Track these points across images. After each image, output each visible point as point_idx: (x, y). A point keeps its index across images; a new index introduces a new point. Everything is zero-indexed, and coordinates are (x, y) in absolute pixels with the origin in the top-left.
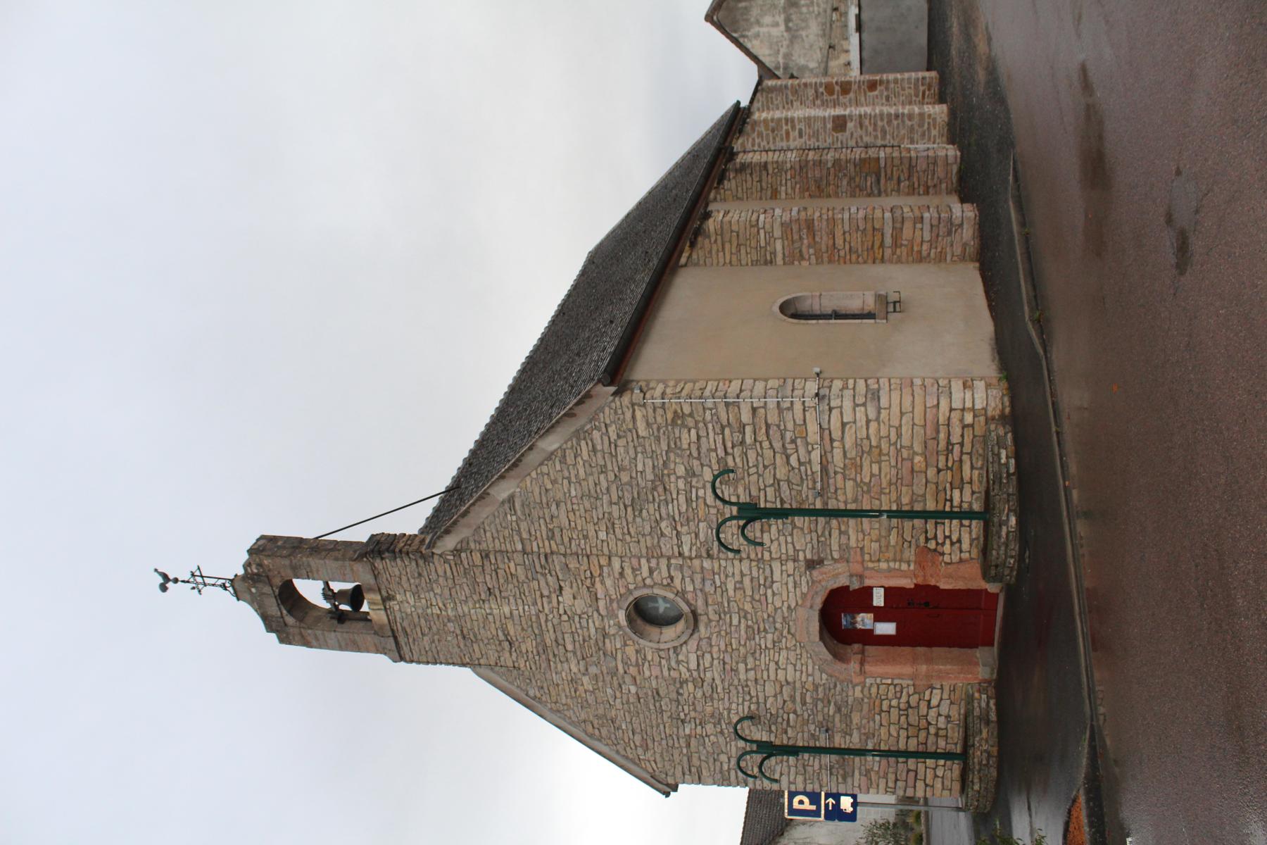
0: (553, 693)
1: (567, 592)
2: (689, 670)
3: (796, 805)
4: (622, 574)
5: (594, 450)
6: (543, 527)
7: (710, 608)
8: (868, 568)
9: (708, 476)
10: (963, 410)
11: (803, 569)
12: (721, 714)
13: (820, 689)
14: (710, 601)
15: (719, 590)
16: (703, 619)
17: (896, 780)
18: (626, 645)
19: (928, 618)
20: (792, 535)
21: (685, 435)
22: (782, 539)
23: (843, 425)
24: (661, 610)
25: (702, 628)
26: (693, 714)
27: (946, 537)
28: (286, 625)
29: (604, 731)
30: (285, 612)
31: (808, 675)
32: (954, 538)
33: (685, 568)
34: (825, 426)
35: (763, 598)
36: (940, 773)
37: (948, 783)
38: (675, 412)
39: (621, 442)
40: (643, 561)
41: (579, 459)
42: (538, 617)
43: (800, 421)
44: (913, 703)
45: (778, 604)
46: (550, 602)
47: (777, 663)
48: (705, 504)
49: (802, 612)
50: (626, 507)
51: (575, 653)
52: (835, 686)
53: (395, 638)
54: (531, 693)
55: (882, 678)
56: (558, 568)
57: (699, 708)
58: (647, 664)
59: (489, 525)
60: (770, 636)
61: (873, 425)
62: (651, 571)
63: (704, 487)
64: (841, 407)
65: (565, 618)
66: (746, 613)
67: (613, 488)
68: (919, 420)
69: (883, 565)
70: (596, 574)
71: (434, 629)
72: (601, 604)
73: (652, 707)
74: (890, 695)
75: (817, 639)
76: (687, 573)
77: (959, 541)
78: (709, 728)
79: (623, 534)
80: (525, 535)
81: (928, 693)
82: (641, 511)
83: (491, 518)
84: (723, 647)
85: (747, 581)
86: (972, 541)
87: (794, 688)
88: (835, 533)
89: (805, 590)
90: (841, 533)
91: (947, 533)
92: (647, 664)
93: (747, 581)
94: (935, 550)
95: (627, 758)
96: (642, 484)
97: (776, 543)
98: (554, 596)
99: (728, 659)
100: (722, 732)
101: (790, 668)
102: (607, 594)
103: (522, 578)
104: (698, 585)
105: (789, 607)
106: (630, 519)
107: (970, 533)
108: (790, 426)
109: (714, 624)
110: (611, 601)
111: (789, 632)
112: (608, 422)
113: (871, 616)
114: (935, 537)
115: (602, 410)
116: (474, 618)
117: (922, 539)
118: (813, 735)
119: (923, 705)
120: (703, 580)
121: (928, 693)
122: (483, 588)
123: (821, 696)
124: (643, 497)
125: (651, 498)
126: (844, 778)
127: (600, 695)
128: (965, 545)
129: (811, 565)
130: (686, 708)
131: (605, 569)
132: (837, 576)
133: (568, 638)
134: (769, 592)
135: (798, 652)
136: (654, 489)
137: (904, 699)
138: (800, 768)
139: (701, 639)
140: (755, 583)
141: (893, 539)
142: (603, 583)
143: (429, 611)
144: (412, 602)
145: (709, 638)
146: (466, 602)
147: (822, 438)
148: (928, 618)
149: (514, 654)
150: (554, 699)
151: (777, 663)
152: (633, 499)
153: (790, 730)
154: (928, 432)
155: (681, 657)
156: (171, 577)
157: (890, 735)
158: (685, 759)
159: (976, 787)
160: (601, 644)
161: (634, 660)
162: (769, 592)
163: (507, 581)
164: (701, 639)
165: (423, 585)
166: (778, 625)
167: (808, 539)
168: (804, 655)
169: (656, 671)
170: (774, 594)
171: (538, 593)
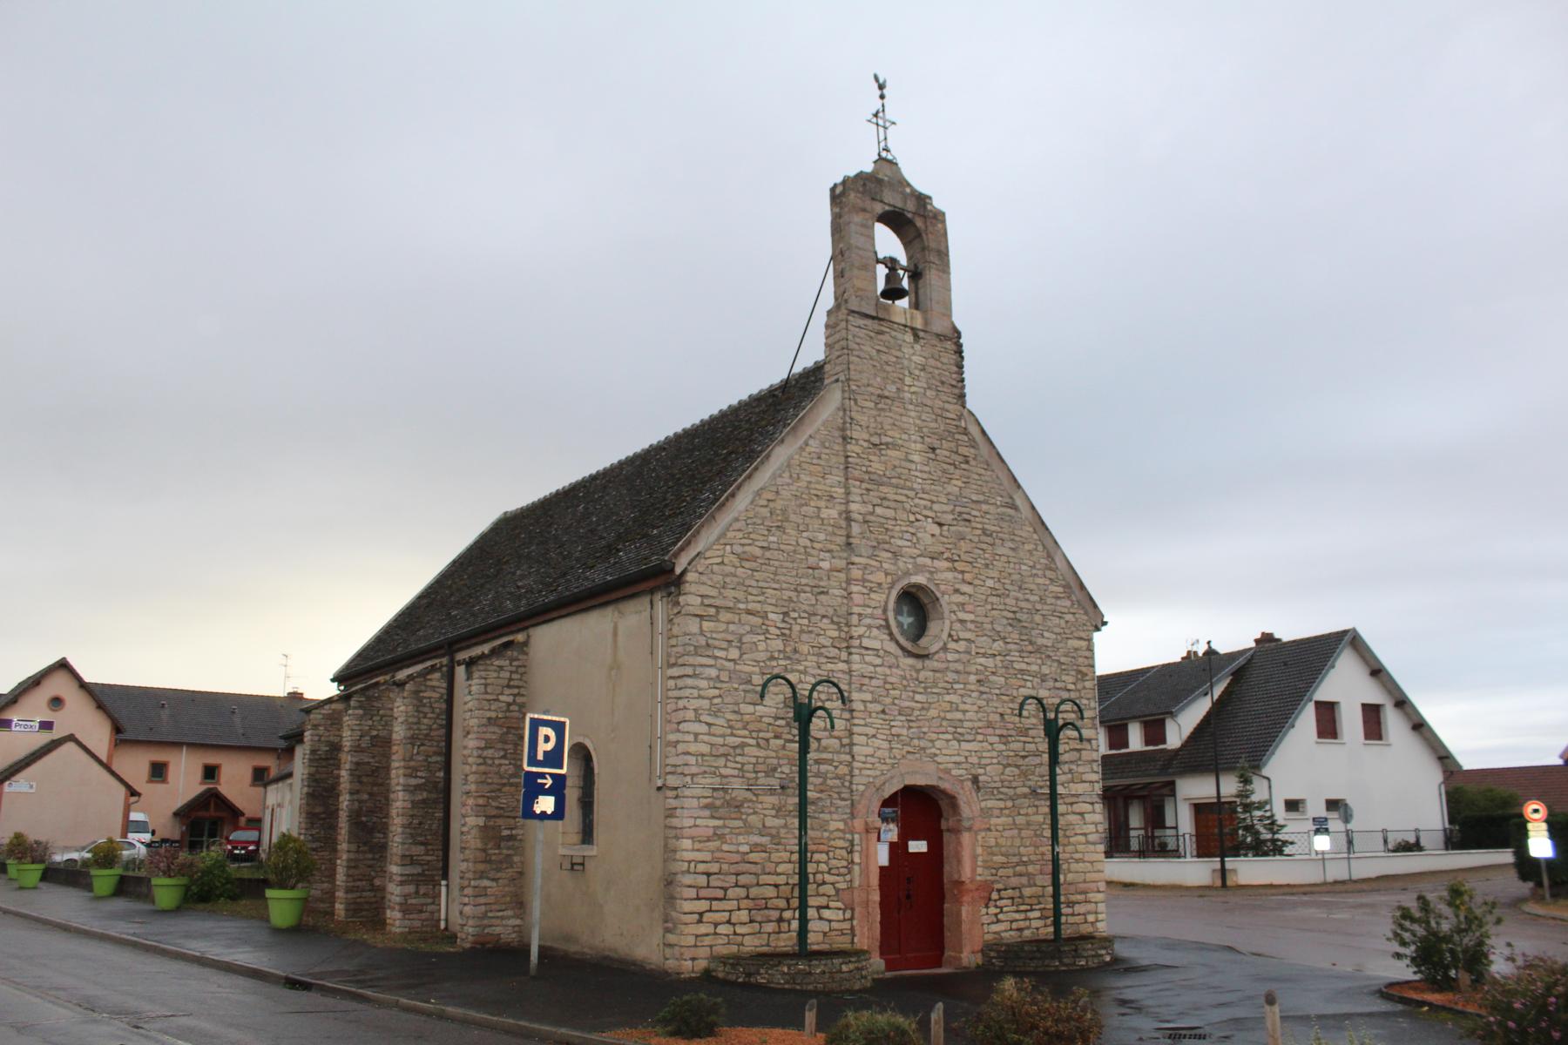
0: (812, 468)
1: (936, 530)
2: (860, 637)
4: (957, 591)
8: (976, 833)
9: (1042, 693)
12: (799, 662)
16: (918, 664)
17: (708, 874)
19: (917, 895)
21: (1071, 679)
22: (995, 754)
23: (1081, 814)
24: (910, 620)
25: (911, 661)
26: (796, 628)
29: (765, 512)
36: (722, 929)
37: (707, 941)
40: (971, 617)
42: (912, 489)
43: (1085, 777)
44: (822, 889)
49: (932, 768)
51: (872, 513)
54: (811, 442)
57: (805, 637)
60: (904, 732)
62: (962, 622)
65: (912, 518)
68: (1089, 877)
69: (979, 850)
71: (888, 369)
72: (928, 561)
73: (804, 581)
74: (834, 862)
75: (908, 782)
76: (965, 657)
77: (998, 921)
78: (777, 644)
80: (984, 507)
81: (839, 905)
85: (959, 715)
87: (839, 752)
88: (1001, 804)
89: (954, 772)
93: (959, 715)
96: (1034, 632)
99: (874, 682)
100: (772, 658)
101: (869, 750)
102: (937, 571)
103: (950, 489)
104: (953, 666)
106: (1005, 613)
108: (1081, 769)
115: (1086, 613)
117: (1000, 886)
118: (775, 770)
119: (822, 901)
120: (957, 672)
121: (839, 905)
122: (936, 444)
126: (706, 807)
127: (816, 524)
128: (995, 928)
129: (975, 780)
130: (805, 622)
132: (970, 805)
134: (949, 737)
136: (1031, 643)
137: (828, 878)
138: (722, 750)
141: (1000, 859)
142: (949, 570)
144: (914, 358)
148: (917, 895)
150: (805, 466)
153: (780, 742)
155: (875, 632)
157: (778, 864)
159: (844, 968)
161: (870, 577)
162: (949, 737)
163: (944, 471)
166: (916, 742)
169: (857, 598)
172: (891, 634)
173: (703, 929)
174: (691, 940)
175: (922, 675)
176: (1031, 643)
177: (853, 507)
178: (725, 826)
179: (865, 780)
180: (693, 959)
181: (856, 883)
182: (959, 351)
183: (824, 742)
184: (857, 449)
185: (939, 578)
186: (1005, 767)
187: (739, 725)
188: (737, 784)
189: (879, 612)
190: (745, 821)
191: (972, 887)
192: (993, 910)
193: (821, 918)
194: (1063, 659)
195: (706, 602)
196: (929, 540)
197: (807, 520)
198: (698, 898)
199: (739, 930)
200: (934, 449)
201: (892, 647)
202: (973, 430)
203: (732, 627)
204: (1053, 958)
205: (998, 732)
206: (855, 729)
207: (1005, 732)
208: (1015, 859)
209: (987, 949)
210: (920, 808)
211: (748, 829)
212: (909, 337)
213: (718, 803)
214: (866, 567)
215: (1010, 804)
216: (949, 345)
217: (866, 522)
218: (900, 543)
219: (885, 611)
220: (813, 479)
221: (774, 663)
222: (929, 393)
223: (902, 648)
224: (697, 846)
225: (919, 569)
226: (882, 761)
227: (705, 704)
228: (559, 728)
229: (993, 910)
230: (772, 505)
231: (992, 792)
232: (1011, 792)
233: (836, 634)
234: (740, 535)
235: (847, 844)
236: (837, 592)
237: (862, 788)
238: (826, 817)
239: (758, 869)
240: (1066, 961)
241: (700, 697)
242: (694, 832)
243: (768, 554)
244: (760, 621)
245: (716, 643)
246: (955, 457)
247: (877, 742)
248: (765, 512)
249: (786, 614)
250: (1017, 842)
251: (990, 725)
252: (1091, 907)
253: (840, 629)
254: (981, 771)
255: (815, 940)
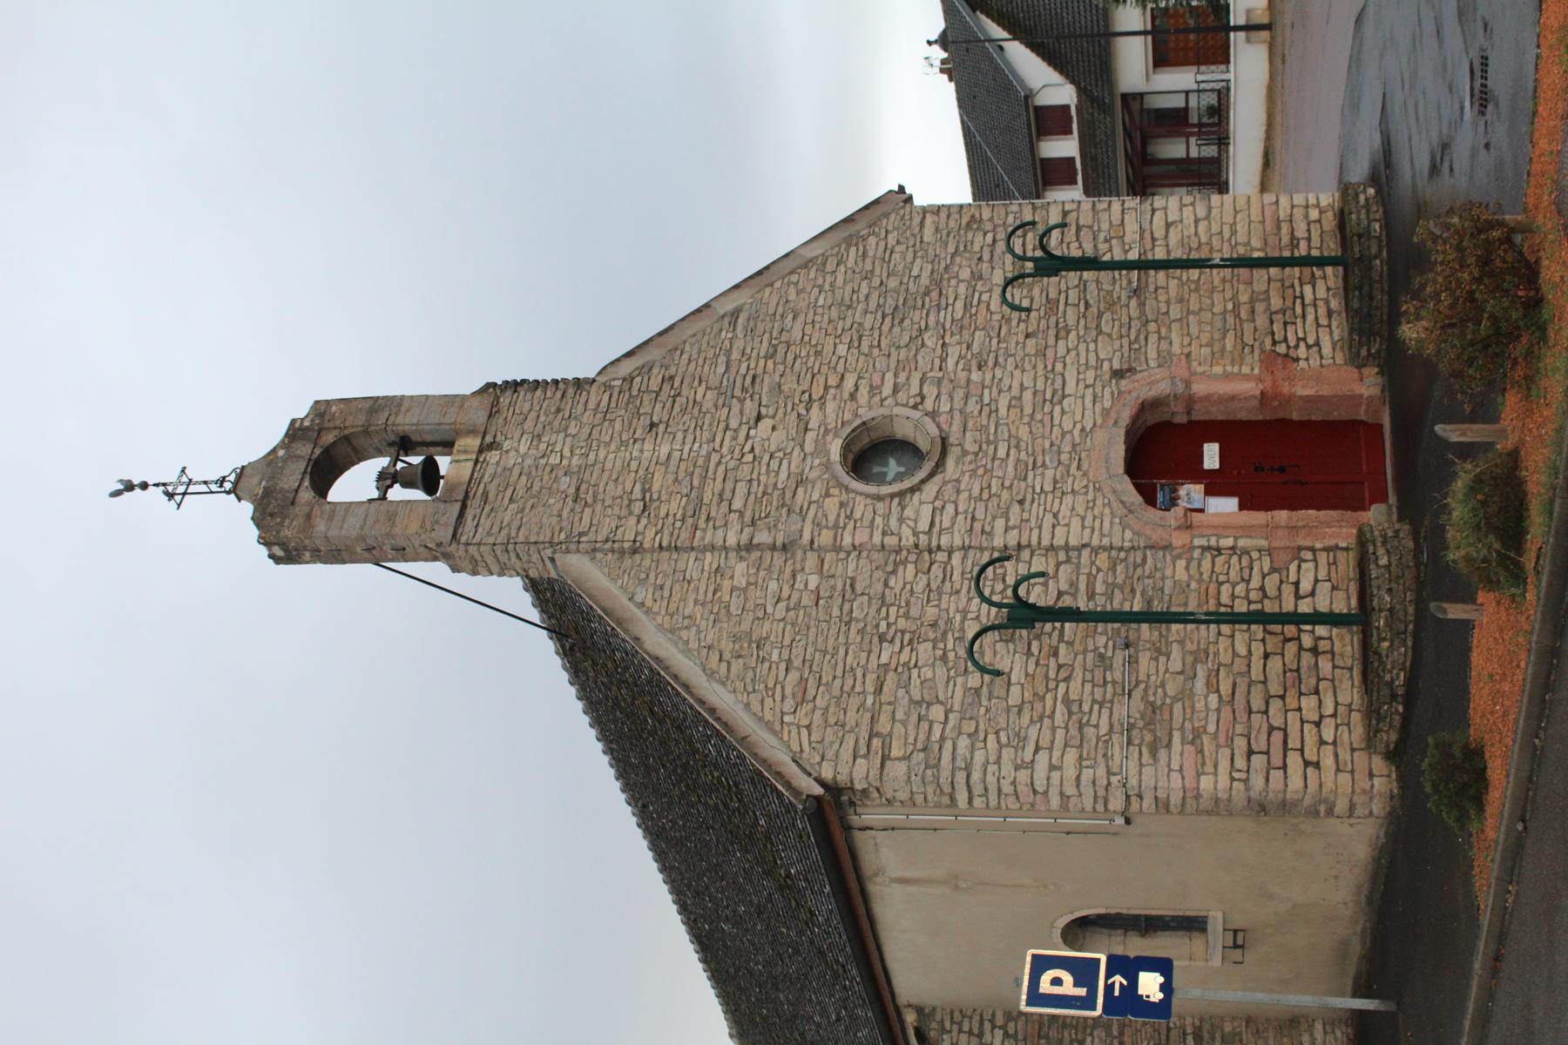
1: (766, 424)
2: (915, 533)
3: (1045, 986)
4: (853, 396)
5: (864, 254)
6: (765, 344)
7: (968, 434)
8: (1193, 374)
9: (998, 278)
10: (1307, 207)
11: (1107, 377)
12: (949, 621)
13: (1119, 568)
14: (970, 425)
15: (986, 409)
16: (954, 452)
17: (1250, 753)
18: (827, 495)
19: (1279, 459)
20: (1095, 341)
21: (979, 238)
22: (1082, 346)
23: (1168, 225)
24: (892, 462)
25: (950, 463)
26: (902, 624)
27: (1299, 339)
28: (293, 503)
29: (737, 666)
30: (306, 483)
31: (1102, 535)
32: (1311, 341)
33: (945, 382)
34: (1146, 226)
35: (1047, 419)
36: (1328, 735)
37: (1345, 755)
38: (973, 216)
39: (898, 248)
40: (889, 376)
41: (842, 268)
43: (1116, 221)
44: (1271, 591)
45: (1067, 426)
46: (735, 439)
47: (1055, 516)
48: (988, 309)
49: (1100, 435)
50: (883, 317)
51: (741, 514)
52: (1144, 560)
53: (464, 507)
54: (639, 598)
55: (1219, 537)
56: (765, 389)
57: (914, 612)
58: (851, 525)
59: (692, 346)
60: (1049, 473)
61: (1202, 226)
62: (896, 390)
63: (990, 291)
64: (1165, 208)
65: (749, 458)
66: (1019, 440)
67: (875, 296)
69: (1218, 370)
70: (815, 397)
71: (536, 488)
72: (810, 436)
73: (836, 612)
74: (1232, 574)
75: (1121, 470)
77: (1317, 344)
78: (924, 649)
79: (871, 346)
80: (735, 355)
81: (1293, 567)
82: (902, 321)
83: (699, 336)
84: (976, 492)
85: (1028, 395)
86: (1334, 345)
88: (1153, 338)
89: (1107, 404)
90: (1160, 338)
91: (1301, 335)
92: (851, 525)
93: (1028, 395)
94: (1286, 355)
95: (761, 719)
96: (912, 288)
97: (1073, 353)
98: (744, 428)
99: (980, 514)
100: (944, 658)
101: (1076, 523)
102: (823, 423)
103: (708, 404)
104: (958, 404)
105: (1083, 429)
106: (885, 328)
107: (1331, 333)
108: (1105, 226)
109: (969, 458)
110: (827, 432)
111: (1079, 468)
112: (890, 228)
113: (1201, 487)
114: (1286, 340)
115: (887, 215)
116: (608, 466)
117: (1268, 341)
118: (1102, 656)
119: (1288, 591)
120: (967, 397)
121: (1293, 567)
123: (1119, 580)
124: (910, 302)
125: (919, 303)
126: (1154, 753)
127: (755, 595)
128: (1327, 349)
129: (1118, 374)
130: (893, 610)
131: (832, 391)
132: (1154, 382)
133: (741, 489)
134: (1057, 409)
135: (1090, 497)
136: (927, 293)
138: (1074, 731)
139: (945, 483)
140: (1039, 398)
141: (1229, 342)
142: (823, 406)
143: (543, 461)
144: (523, 449)
145: (958, 481)
146: (608, 444)
147: (1142, 238)
148: (1279, 459)
149: (644, 521)
150: (672, 608)
151: (1055, 516)
152: (896, 308)
153: (1063, 648)
154: (1268, 228)
155: (908, 512)
156: (136, 482)
157: (1235, 654)
158: (868, 715)
159: (1383, 561)
160: (788, 495)
161: (832, 518)
162: (1057, 409)
163: (684, 411)
164: (945, 483)
165: (556, 423)
166: (1064, 457)
167: (1117, 344)
168: (1099, 502)
169: (862, 537)
170: (1063, 412)
171: (722, 425)
172: (912, 490)
173: (1328, 762)
174: (1344, 778)
175: (970, 446)
176: (927, 293)
177: (732, 540)
178: (1182, 728)
179: (1117, 529)
180: (1371, 775)
181: (1263, 543)
182: (515, 385)
183: (1064, 586)
184: (650, 533)
185: (832, 422)
186: (1100, 332)
187: (1038, 706)
188: (1120, 711)
189: (880, 506)
190: (1175, 699)
191: (1268, 383)
192: (1302, 352)
193: (1312, 594)
194: (951, 249)
195: (863, 751)
196: (780, 434)
197: (750, 605)
198: (1284, 767)
199: (1329, 710)
200: (652, 425)
201: (930, 489)
202: (626, 368)
203: (900, 715)
204: (1370, 268)
205: (1051, 341)
206: (1046, 542)
207: (1052, 332)
208: (1230, 319)
209: (1356, 360)
210: (1159, 452)
211: (1186, 695)
212: (493, 456)
213: (1148, 738)
214: (817, 524)
215: (1152, 327)
216: (505, 400)
217: (753, 523)
218: (783, 475)
219: (879, 498)
220: (692, 597)
221: (951, 655)
222: (572, 431)
223: (931, 475)
224: (1209, 768)
225: (821, 449)
226: (1090, 505)
227: (1007, 754)
228: (1041, 964)
229: (1302, 352)
230: (727, 656)
231: (1136, 348)
232: (1136, 324)
233: (911, 568)
234: (769, 701)
235: (1208, 556)
236: (852, 566)
237: (1128, 534)
238: (1169, 583)
239: (1242, 684)
240: (1374, 250)
241: (998, 762)
242: (1190, 773)
243: (797, 662)
244: (891, 674)
245: (922, 737)
246: (663, 397)
247: (1065, 511)
248: (737, 666)
249: (882, 638)
250: (1206, 316)
251: (1041, 353)
252: (1298, 214)
253: (905, 562)
254: (1106, 365)
255: (1344, 603)
